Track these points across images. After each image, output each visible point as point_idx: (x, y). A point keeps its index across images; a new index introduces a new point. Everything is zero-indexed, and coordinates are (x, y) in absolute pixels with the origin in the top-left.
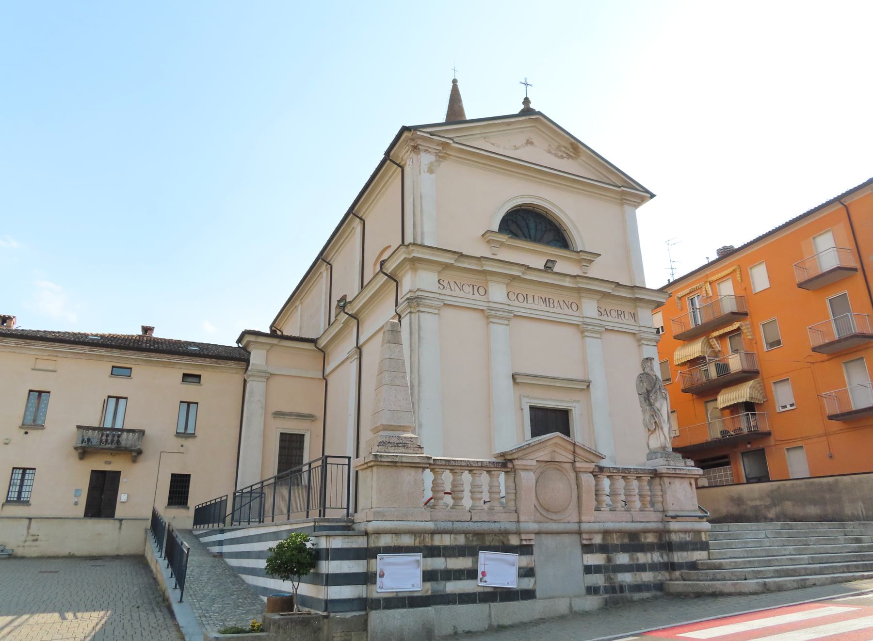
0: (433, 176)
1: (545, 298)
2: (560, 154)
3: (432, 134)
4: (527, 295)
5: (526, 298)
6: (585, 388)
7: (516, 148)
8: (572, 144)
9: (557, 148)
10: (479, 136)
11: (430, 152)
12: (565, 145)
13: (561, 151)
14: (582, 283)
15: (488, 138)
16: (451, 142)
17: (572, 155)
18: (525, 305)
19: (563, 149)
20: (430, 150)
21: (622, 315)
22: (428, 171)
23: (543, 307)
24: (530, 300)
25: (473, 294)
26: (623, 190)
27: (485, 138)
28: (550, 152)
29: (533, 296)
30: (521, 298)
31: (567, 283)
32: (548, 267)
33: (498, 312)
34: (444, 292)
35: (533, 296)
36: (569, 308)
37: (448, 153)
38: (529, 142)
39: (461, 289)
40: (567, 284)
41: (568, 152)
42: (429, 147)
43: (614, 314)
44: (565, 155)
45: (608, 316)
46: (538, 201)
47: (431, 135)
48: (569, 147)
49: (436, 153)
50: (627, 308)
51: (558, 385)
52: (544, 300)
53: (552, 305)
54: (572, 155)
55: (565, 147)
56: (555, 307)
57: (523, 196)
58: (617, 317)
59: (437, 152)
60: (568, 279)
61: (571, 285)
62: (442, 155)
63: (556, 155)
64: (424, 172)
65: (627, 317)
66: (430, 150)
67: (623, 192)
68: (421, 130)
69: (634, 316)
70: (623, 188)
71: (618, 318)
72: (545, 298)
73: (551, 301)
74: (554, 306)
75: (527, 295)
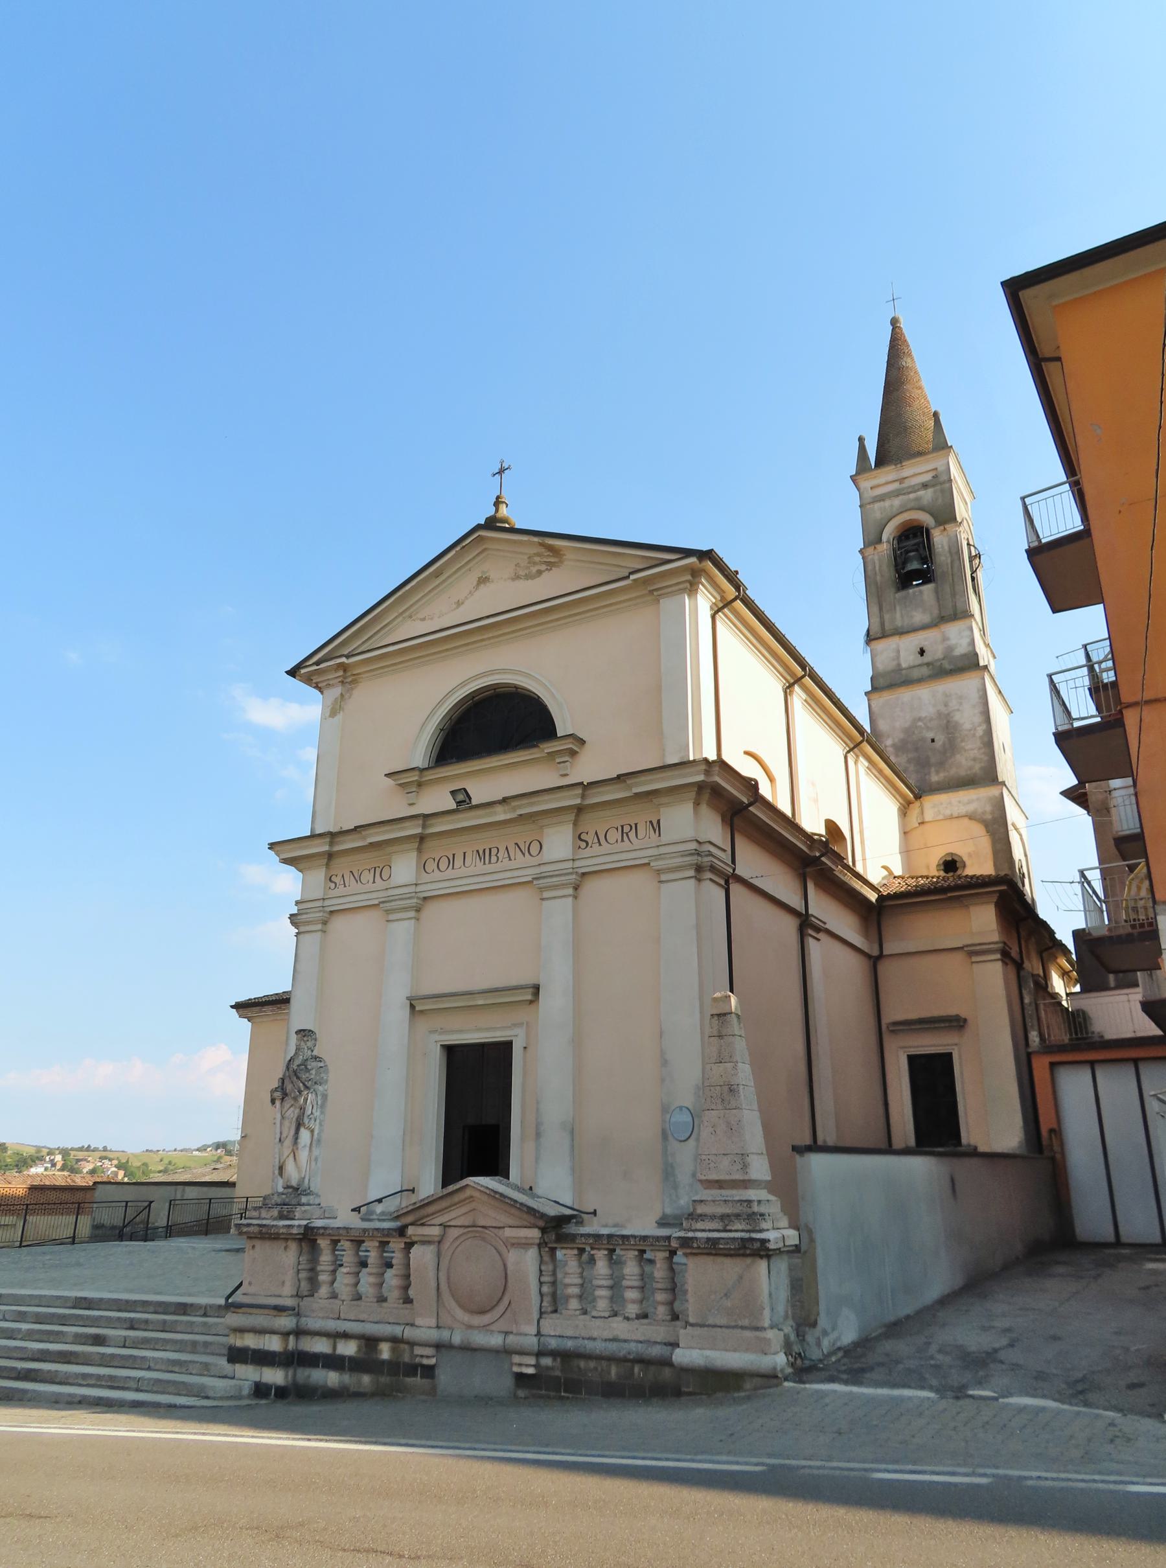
0: (339, 717)
1: (484, 850)
2: (534, 569)
3: (317, 663)
4: (454, 855)
5: (451, 861)
6: (529, 997)
7: (459, 604)
8: (541, 544)
9: (529, 563)
10: (401, 618)
11: (333, 685)
12: (535, 552)
13: (535, 563)
14: (519, 807)
15: (415, 615)
16: (344, 660)
17: (552, 560)
18: (450, 873)
19: (537, 559)
20: (331, 682)
21: (632, 835)
22: (330, 716)
23: (480, 867)
24: (459, 862)
25: (374, 882)
26: (635, 580)
27: (410, 617)
28: (517, 577)
29: (465, 853)
30: (443, 864)
31: (501, 814)
32: (463, 800)
33: (393, 903)
34: (336, 892)
35: (465, 853)
36: (524, 854)
37: (354, 673)
38: (483, 580)
39: (358, 880)
40: (502, 817)
41: (545, 560)
42: (328, 679)
43: (614, 835)
44: (543, 567)
45: (600, 845)
46: (490, 678)
47: (317, 666)
48: (542, 550)
49: (339, 682)
50: (641, 816)
51: (480, 1002)
52: (481, 855)
53: (494, 859)
54: (552, 560)
55: (538, 555)
56: (500, 860)
57: (463, 684)
58: (620, 840)
59: (340, 680)
60: (499, 808)
61: (508, 816)
62: (350, 679)
63: (528, 577)
64: (326, 719)
65: (641, 833)
66: (331, 682)
67: (646, 581)
68: (307, 664)
69: (656, 827)
70: (632, 577)
71: (623, 840)
72: (484, 850)
73: (494, 851)
74: (498, 859)
75: (454, 855)
